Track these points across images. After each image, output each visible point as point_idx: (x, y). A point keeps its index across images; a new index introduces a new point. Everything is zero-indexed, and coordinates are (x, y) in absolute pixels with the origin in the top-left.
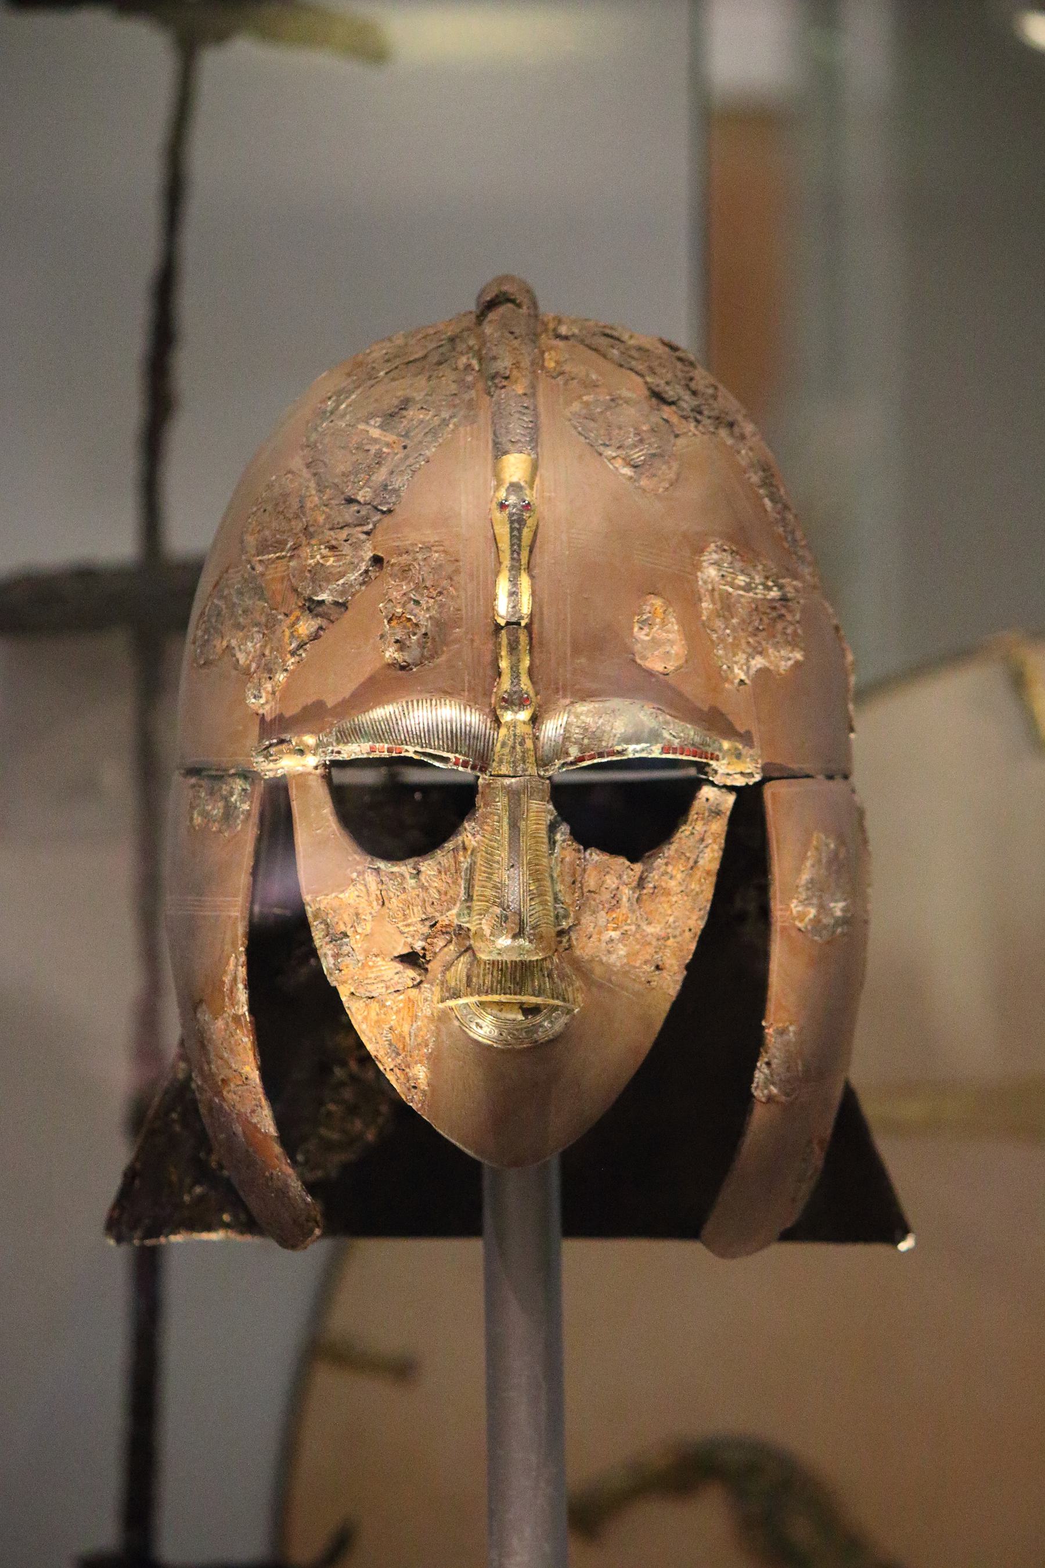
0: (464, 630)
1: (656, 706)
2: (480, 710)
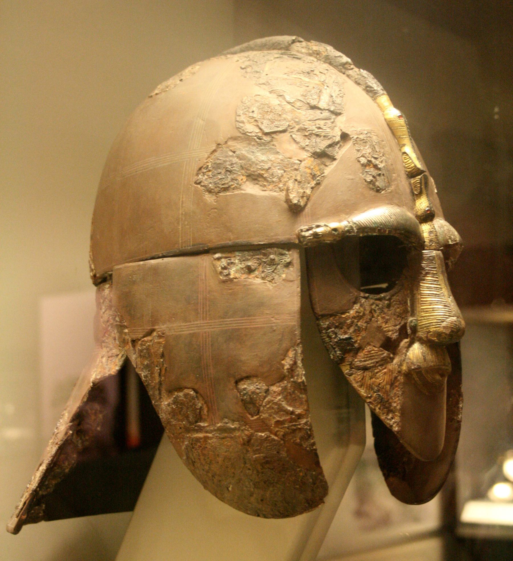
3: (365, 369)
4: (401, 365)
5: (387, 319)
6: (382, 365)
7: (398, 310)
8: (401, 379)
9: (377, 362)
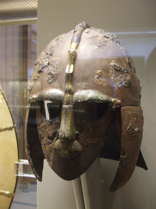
1: (98, 91)
2: (62, 92)
3: (44, 145)
4: (53, 146)
6: (48, 145)
7: (54, 126)
8: (53, 150)
9: (47, 143)
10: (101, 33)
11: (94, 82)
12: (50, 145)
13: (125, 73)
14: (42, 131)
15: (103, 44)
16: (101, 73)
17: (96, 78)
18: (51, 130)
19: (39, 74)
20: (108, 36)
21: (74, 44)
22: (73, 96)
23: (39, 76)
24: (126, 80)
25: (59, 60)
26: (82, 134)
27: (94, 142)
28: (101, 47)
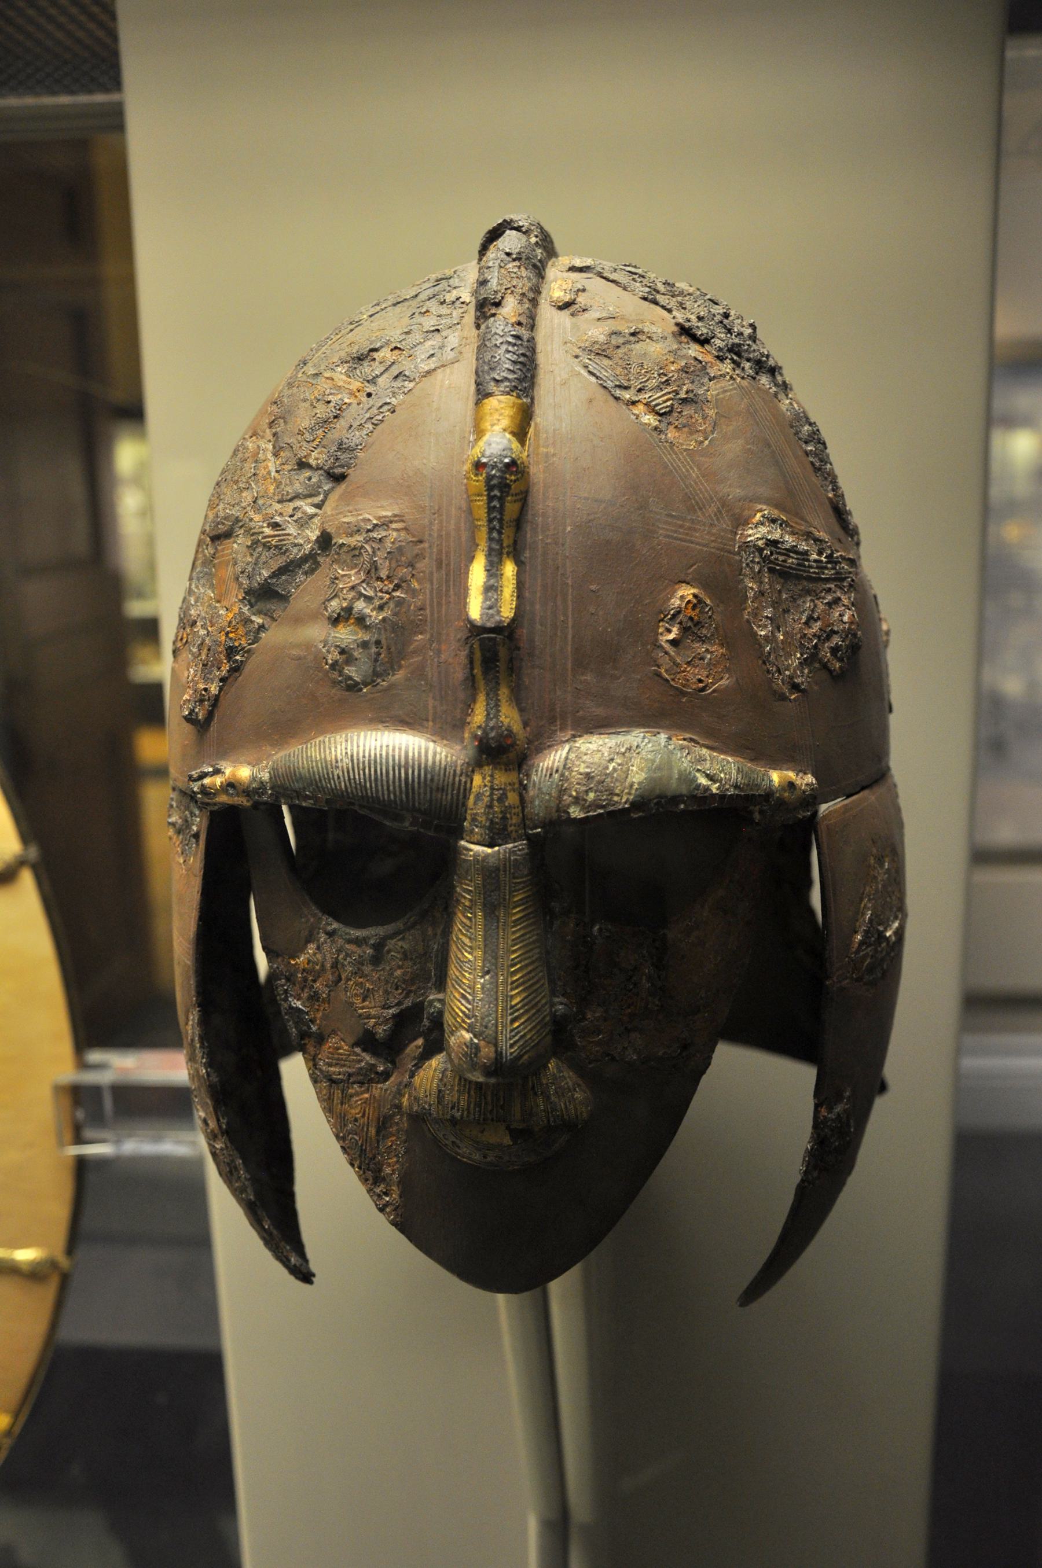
0: (428, 636)
1: (688, 736)
4: (400, 1094)
5: (368, 989)
6: (361, 1083)
7: (398, 972)
9: (350, 1075)
10: (655, 302)
11: (659, 675)
12: (377, 1089)
13: (827, 580)
14: (314, 997)
15: (683, 395)
16: (698, 602)
17: (667, 646)
18: (379, 997)
19: (259, 613)
20: (702, 330)
21: (500, 408)
22: (528, 776)
23: (262, 627)
24: (836, 633)
25: (399, 518)
26: (594, 1014)
27: (660, 1053)
28: (675, 414)
